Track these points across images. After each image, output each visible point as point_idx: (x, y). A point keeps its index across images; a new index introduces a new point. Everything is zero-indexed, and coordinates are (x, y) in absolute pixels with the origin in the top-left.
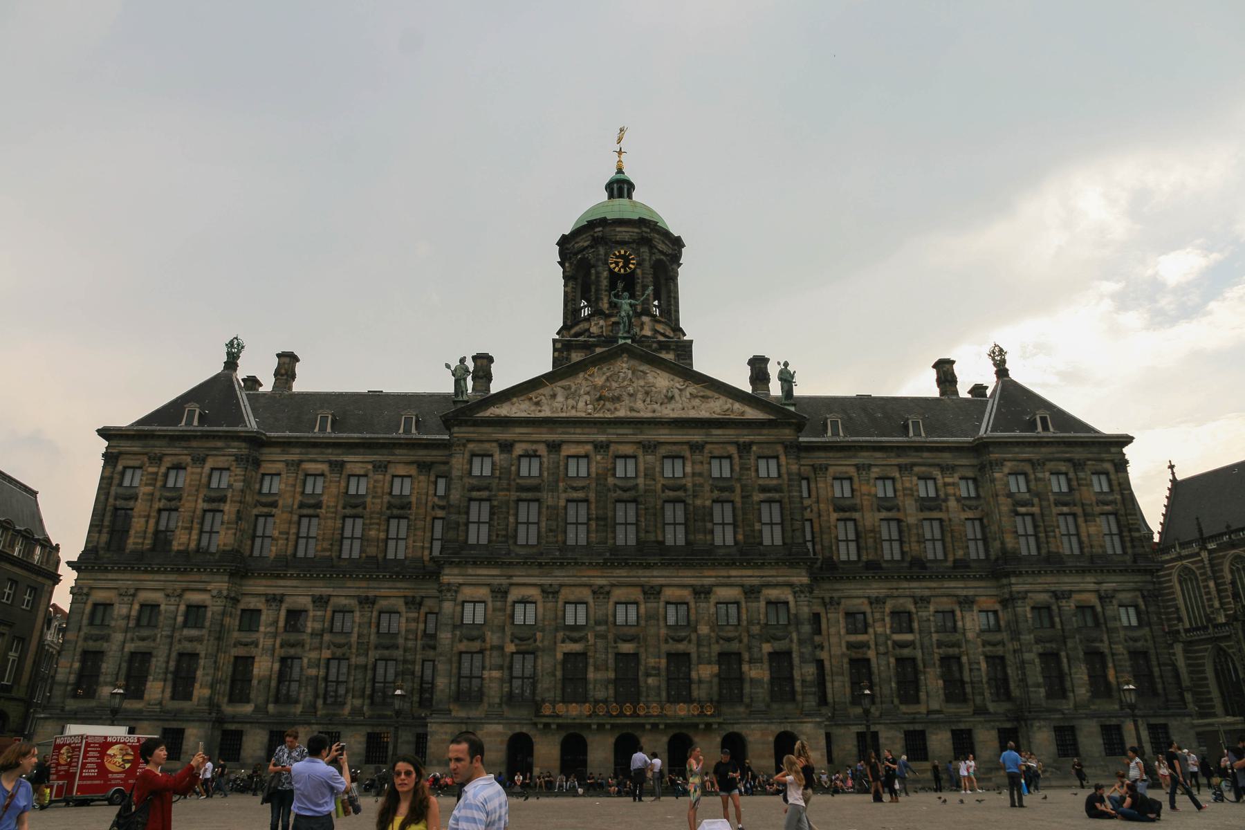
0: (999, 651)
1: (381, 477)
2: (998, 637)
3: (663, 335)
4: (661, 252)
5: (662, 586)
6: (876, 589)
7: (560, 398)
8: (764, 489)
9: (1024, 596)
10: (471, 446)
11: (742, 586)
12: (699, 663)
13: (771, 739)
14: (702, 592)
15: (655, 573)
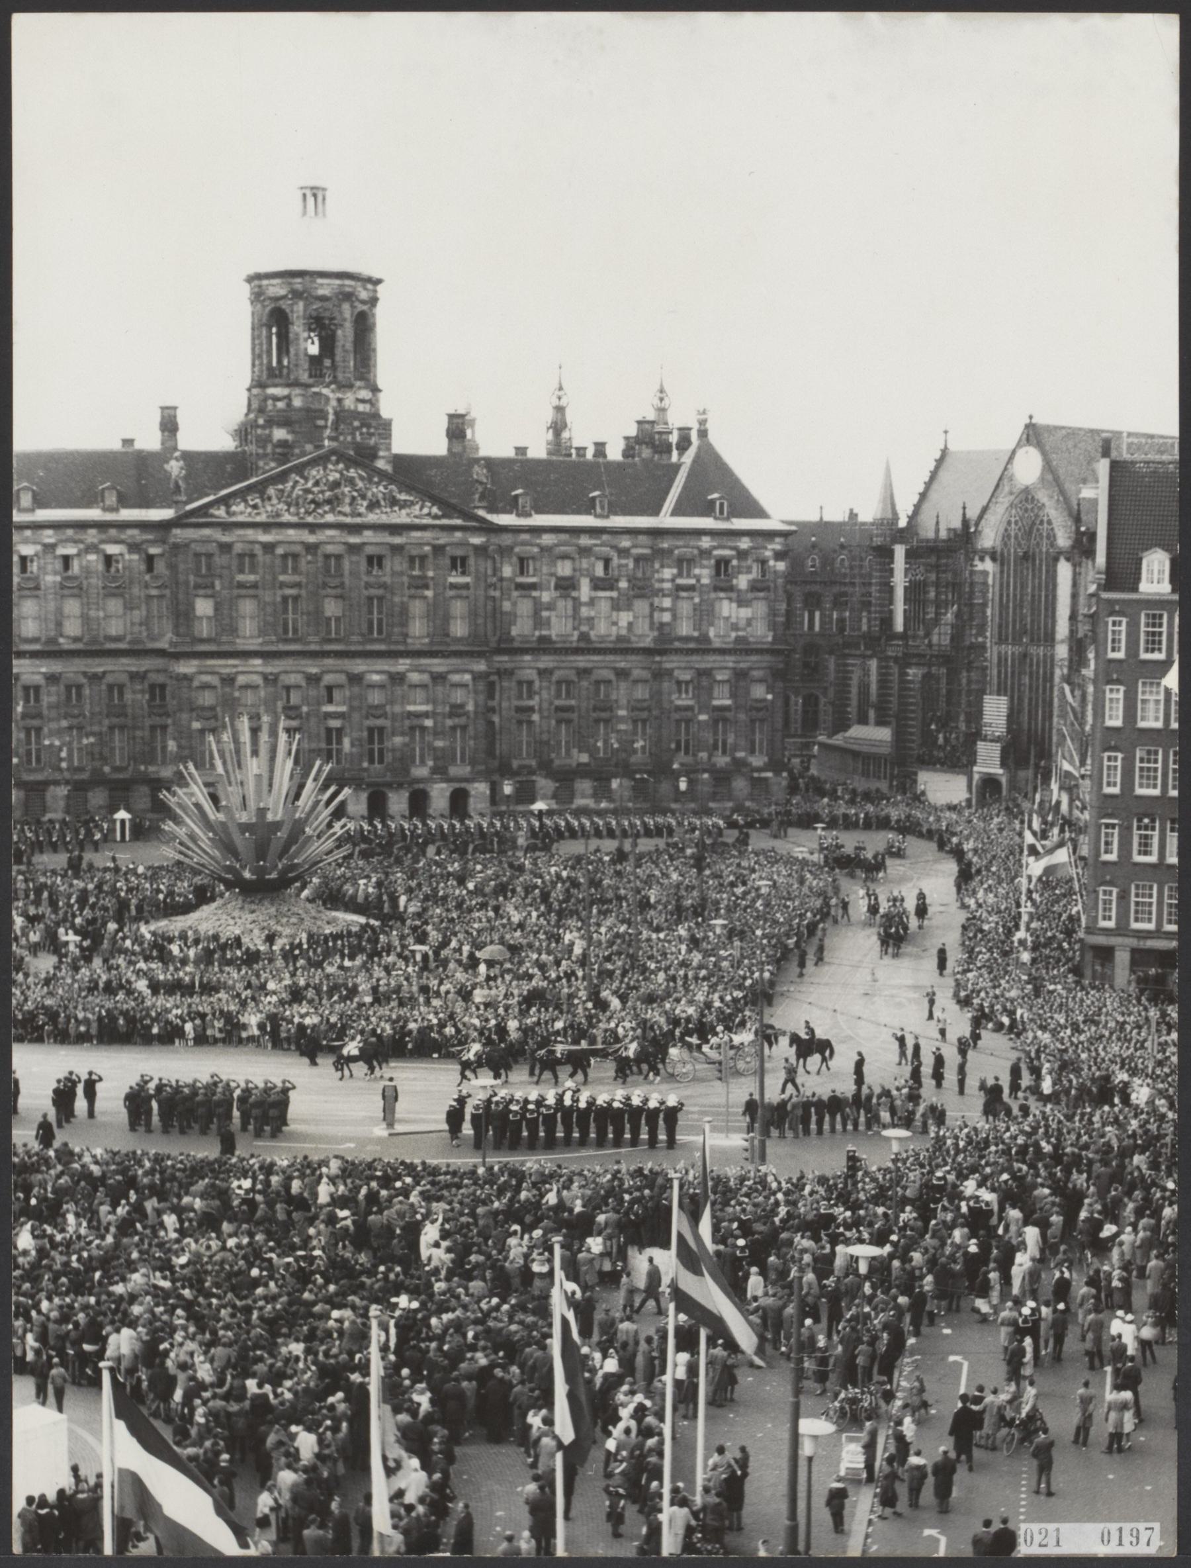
0: (645, 715)
1: (92, 557)
2: (645, 704)
3: (363, 401)
4: (363, 302)
5: (363, 673)
6: (546, 661)
7: (275, 501)
8: (453, 586)
9: (669, 672)
10: (193, 546)
11: (431, 673)
12: (393, 734)
13: (448, 794)
14: (397, 679)
15: (359, 661)
